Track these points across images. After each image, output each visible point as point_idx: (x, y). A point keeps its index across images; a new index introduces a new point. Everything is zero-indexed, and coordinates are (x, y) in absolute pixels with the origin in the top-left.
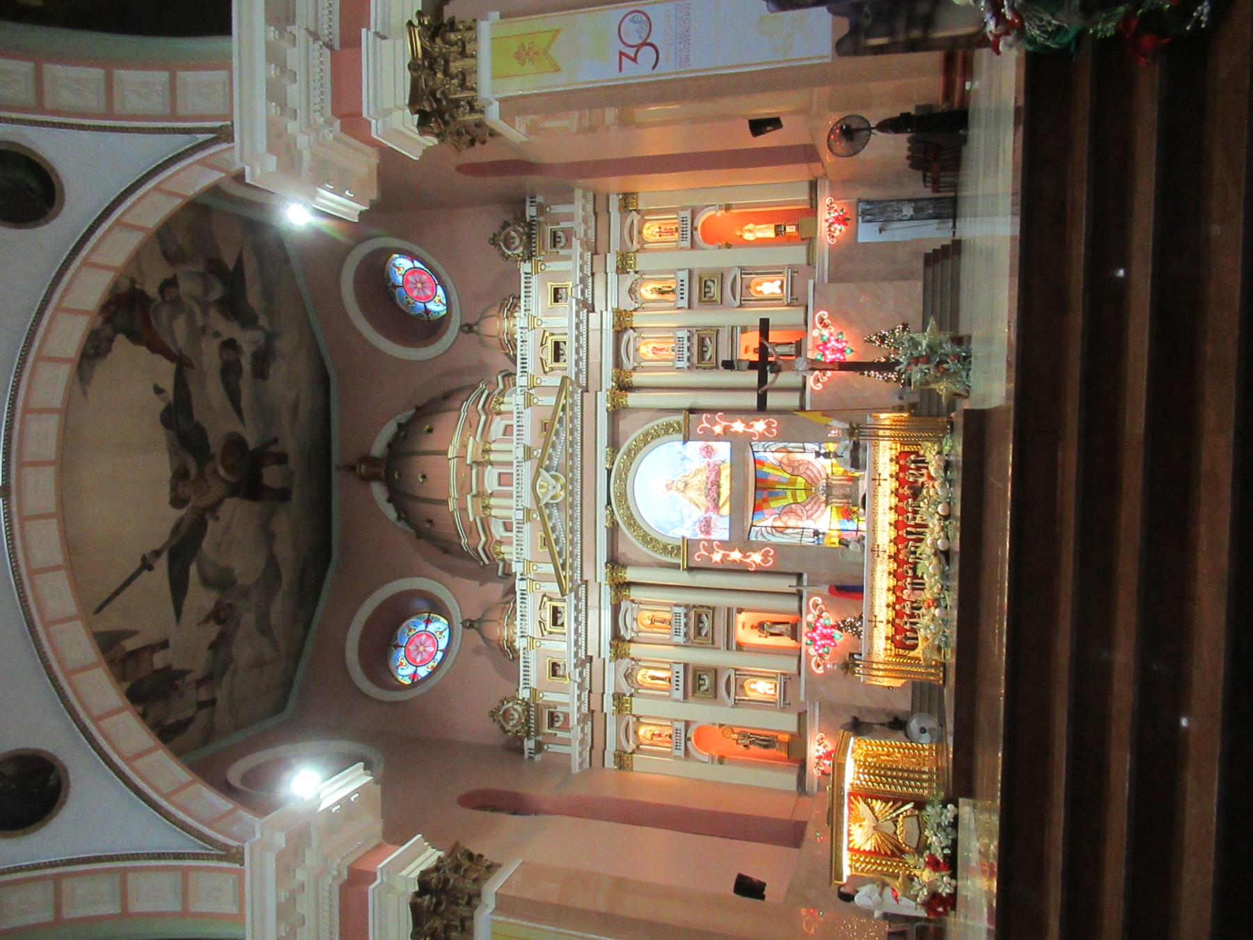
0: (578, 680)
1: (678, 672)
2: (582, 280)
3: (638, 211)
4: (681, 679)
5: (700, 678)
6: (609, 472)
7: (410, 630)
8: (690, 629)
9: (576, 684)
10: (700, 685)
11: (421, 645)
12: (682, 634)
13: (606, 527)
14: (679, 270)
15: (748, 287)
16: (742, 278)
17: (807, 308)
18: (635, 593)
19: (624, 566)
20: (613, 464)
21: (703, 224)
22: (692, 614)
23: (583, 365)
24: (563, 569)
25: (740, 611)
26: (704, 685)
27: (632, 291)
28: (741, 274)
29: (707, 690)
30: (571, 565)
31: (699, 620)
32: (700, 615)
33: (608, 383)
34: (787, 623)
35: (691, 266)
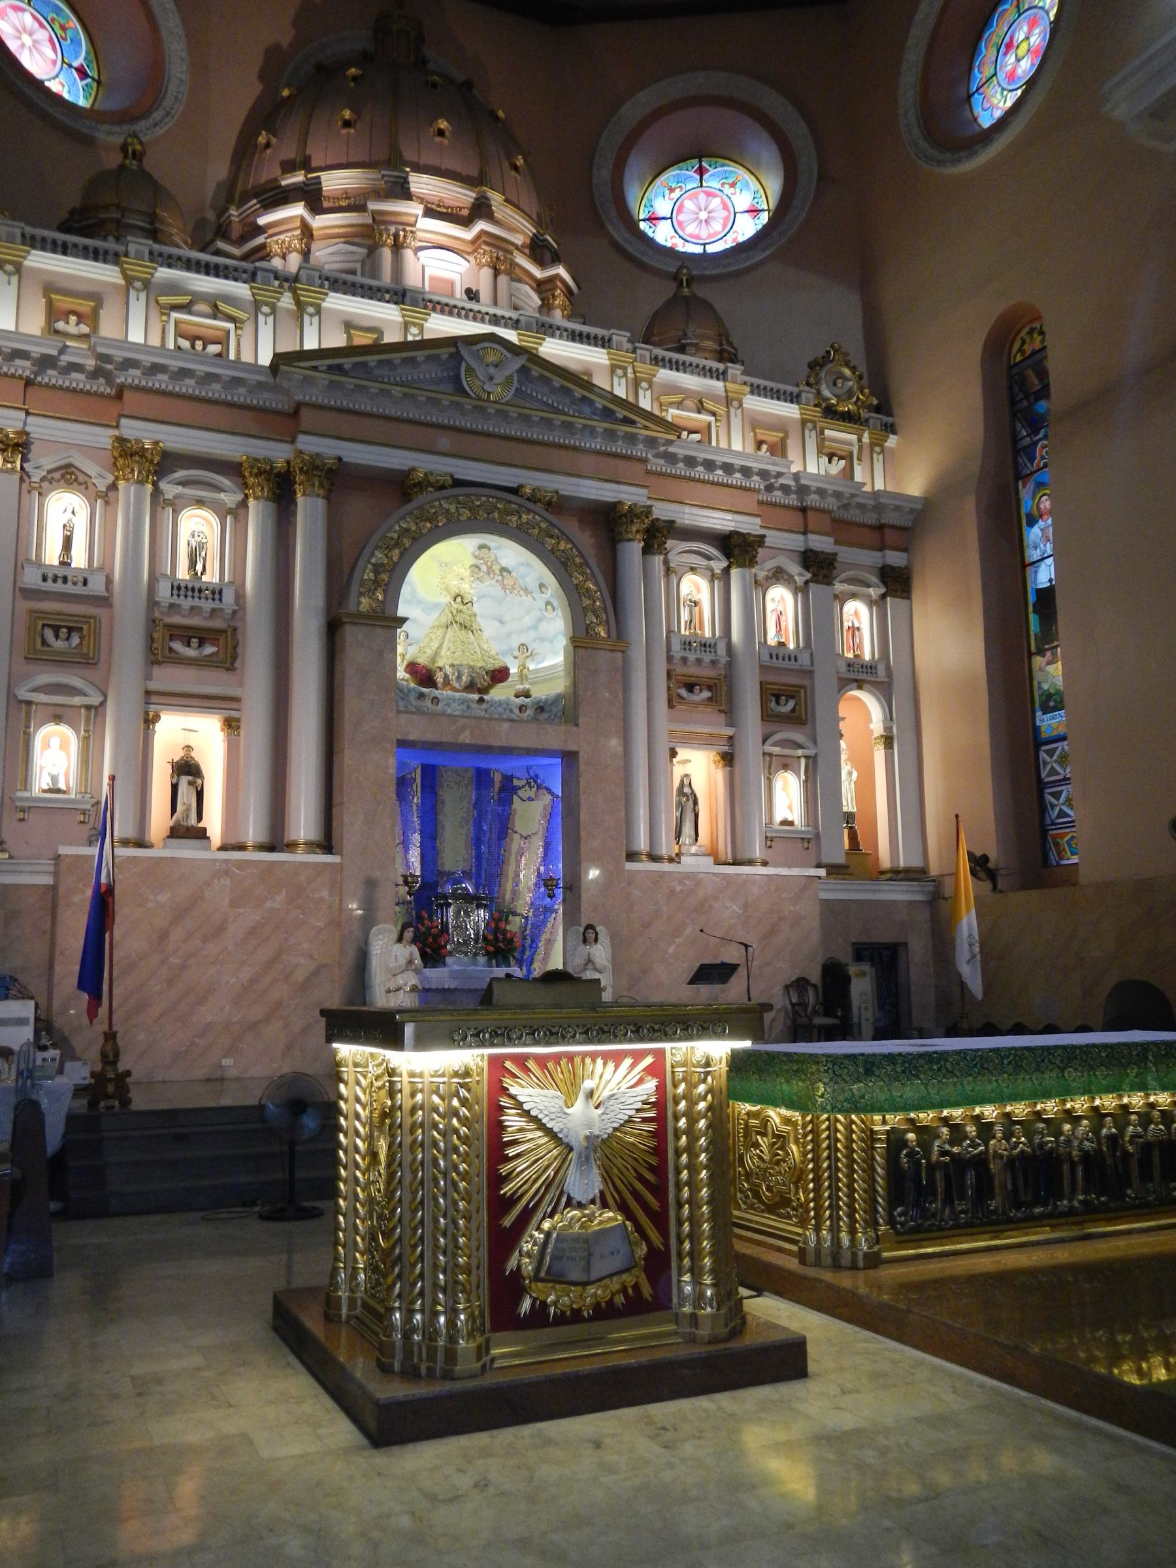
0: (65, 359)
1: (85, 583)
2: (803, 490)
3: (883, 597)
4: (69, 588)
5: (70, 630)
6: (515, 491)
7: (63, 28)
8: (184, 616)
9: (55, 353)
10: (56, 630)
11: (35, 42)
12: (175, 600)
13: (413, 469)
14: (812, 655)
15: (786, 767)
16: (799, 757)
17: (765, 864)
18: (257, 513)
19: (327, 498)
20: (528, 499)
21: (859, 699)
22: (218, 624)
23: (681, 468)
24: (331, 369)
25: (231, 725)
26: (57, 637)
27: (779, 576)
28: (807, 757)
29: (44, 642)
30: (340, 385)
31: (203, 636)
32: (214, 642)
33: (663, 511)
34: (200, 817)
35: (816, 675)
